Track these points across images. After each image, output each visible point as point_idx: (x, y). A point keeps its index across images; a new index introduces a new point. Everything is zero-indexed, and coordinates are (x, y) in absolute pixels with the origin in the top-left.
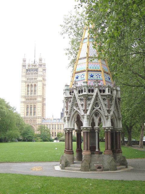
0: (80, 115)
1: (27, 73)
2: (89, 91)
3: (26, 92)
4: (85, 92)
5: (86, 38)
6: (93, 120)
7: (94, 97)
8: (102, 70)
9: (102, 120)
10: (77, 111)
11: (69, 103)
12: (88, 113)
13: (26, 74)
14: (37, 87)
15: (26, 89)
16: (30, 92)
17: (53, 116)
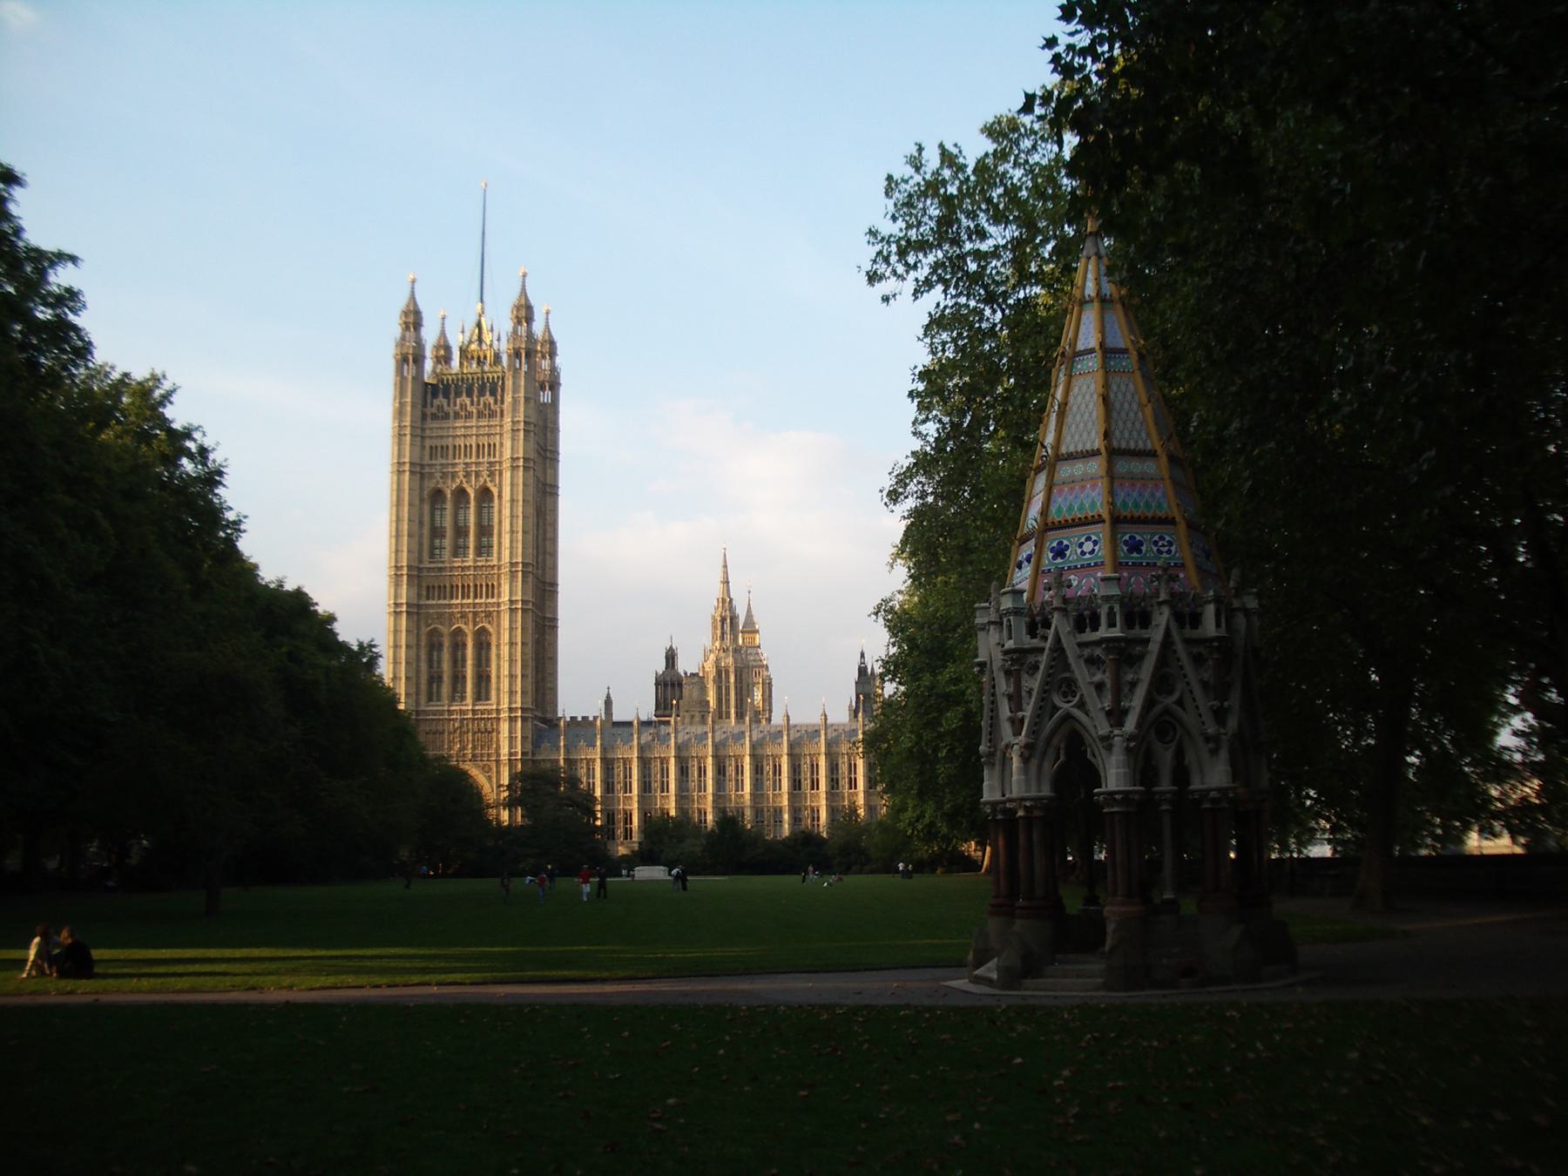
0: (1086, 736)
1: (429, 410)
2: (1129, 622)
3: (426, 541)
4: (1112, 624)
5: (1092, 351)
6: (1149, 755)
7: (1154, 648)
8: (1178, 519)
9: (1190, 757)
10: (1068, 717)
11: (1025, 676)
12: (1130, 725)
13: (424, 417)
14: (496, 501)
15: (427, 519)
16: (447, 542)
17: (608, 703)
